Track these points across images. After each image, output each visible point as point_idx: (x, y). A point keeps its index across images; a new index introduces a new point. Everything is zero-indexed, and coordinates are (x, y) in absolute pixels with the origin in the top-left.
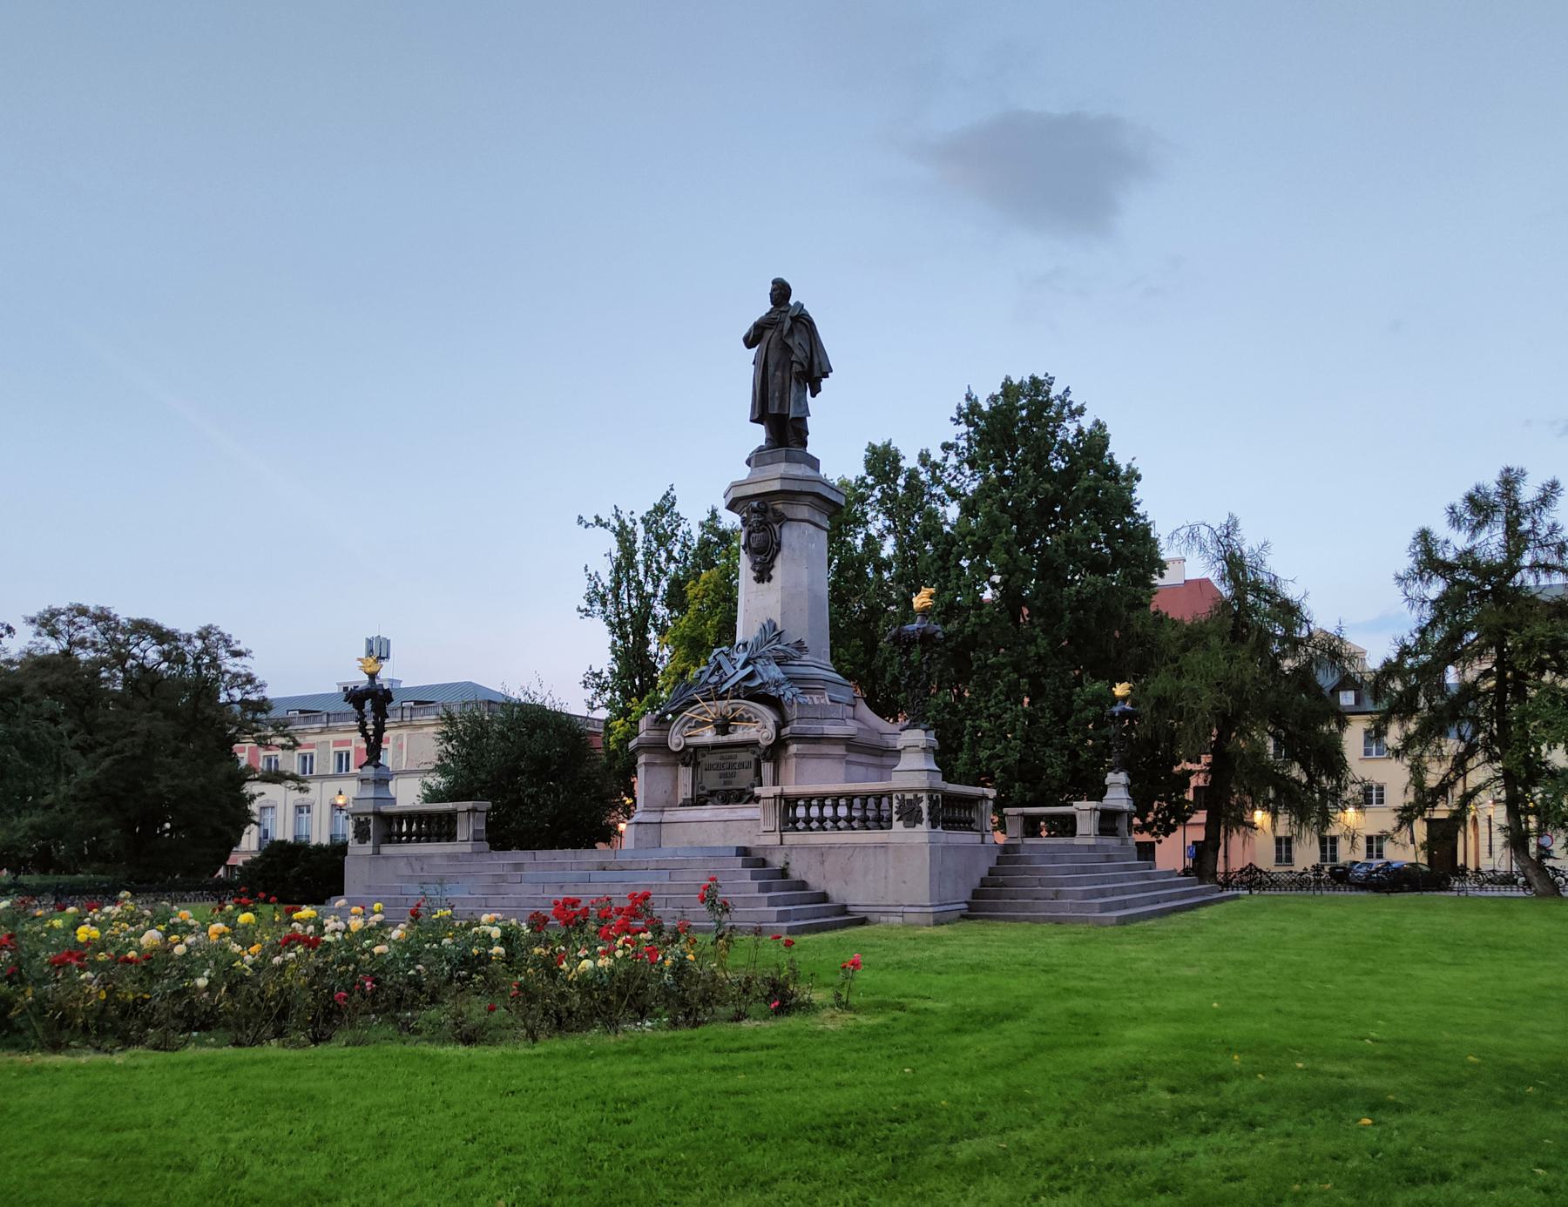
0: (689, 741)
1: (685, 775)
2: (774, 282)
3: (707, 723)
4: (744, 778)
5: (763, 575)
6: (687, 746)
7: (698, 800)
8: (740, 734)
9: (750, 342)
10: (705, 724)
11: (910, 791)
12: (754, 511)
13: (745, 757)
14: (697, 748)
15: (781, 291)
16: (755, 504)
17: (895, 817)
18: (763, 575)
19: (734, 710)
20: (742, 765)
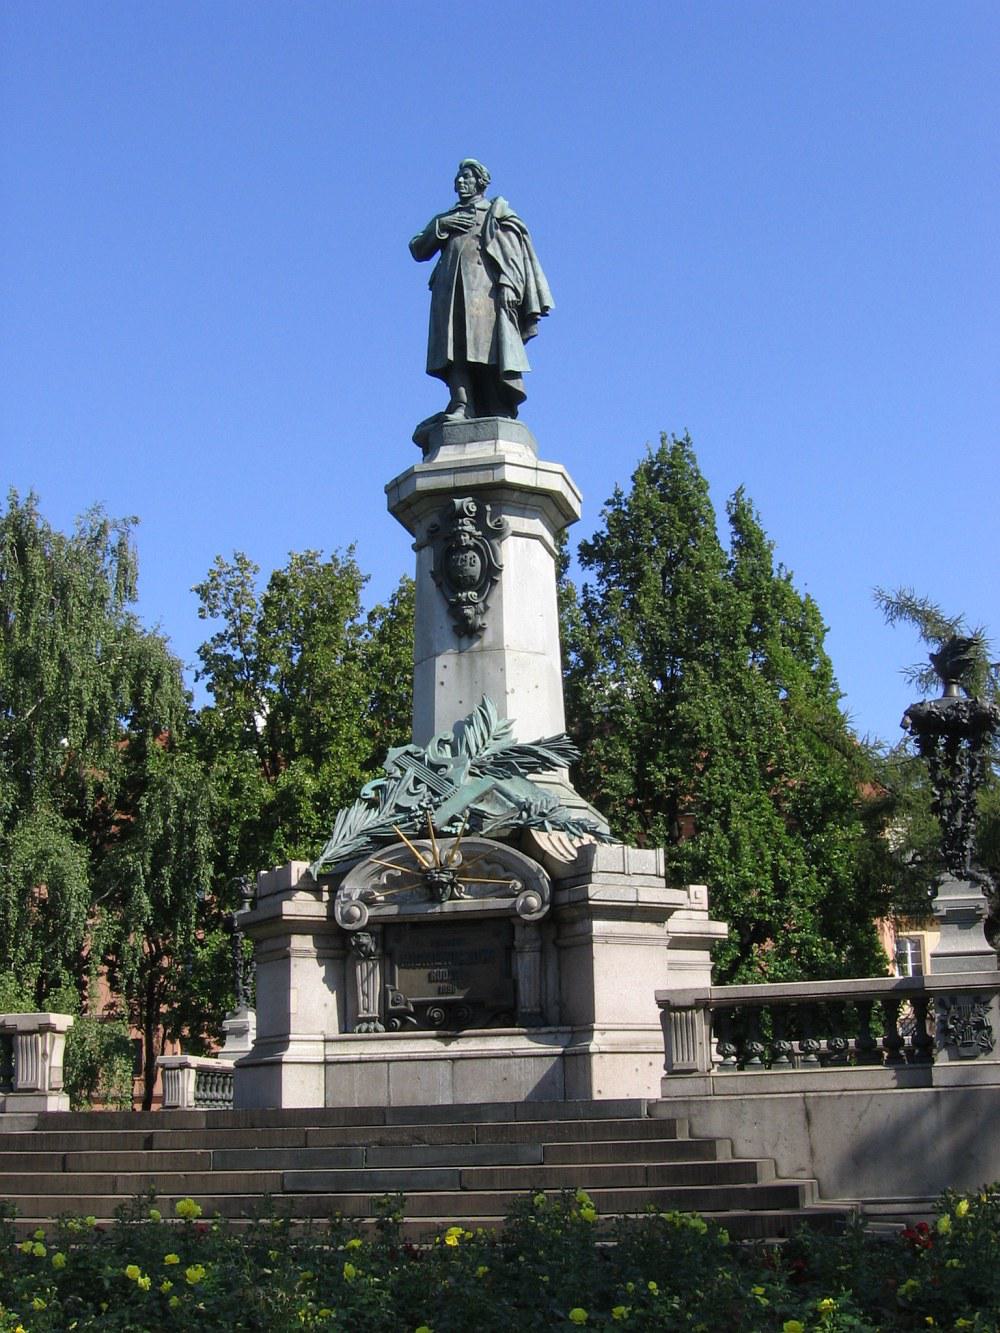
6: (372, 921)
7: (394, 1020)
9: (422, 249)
15: (471, 181)
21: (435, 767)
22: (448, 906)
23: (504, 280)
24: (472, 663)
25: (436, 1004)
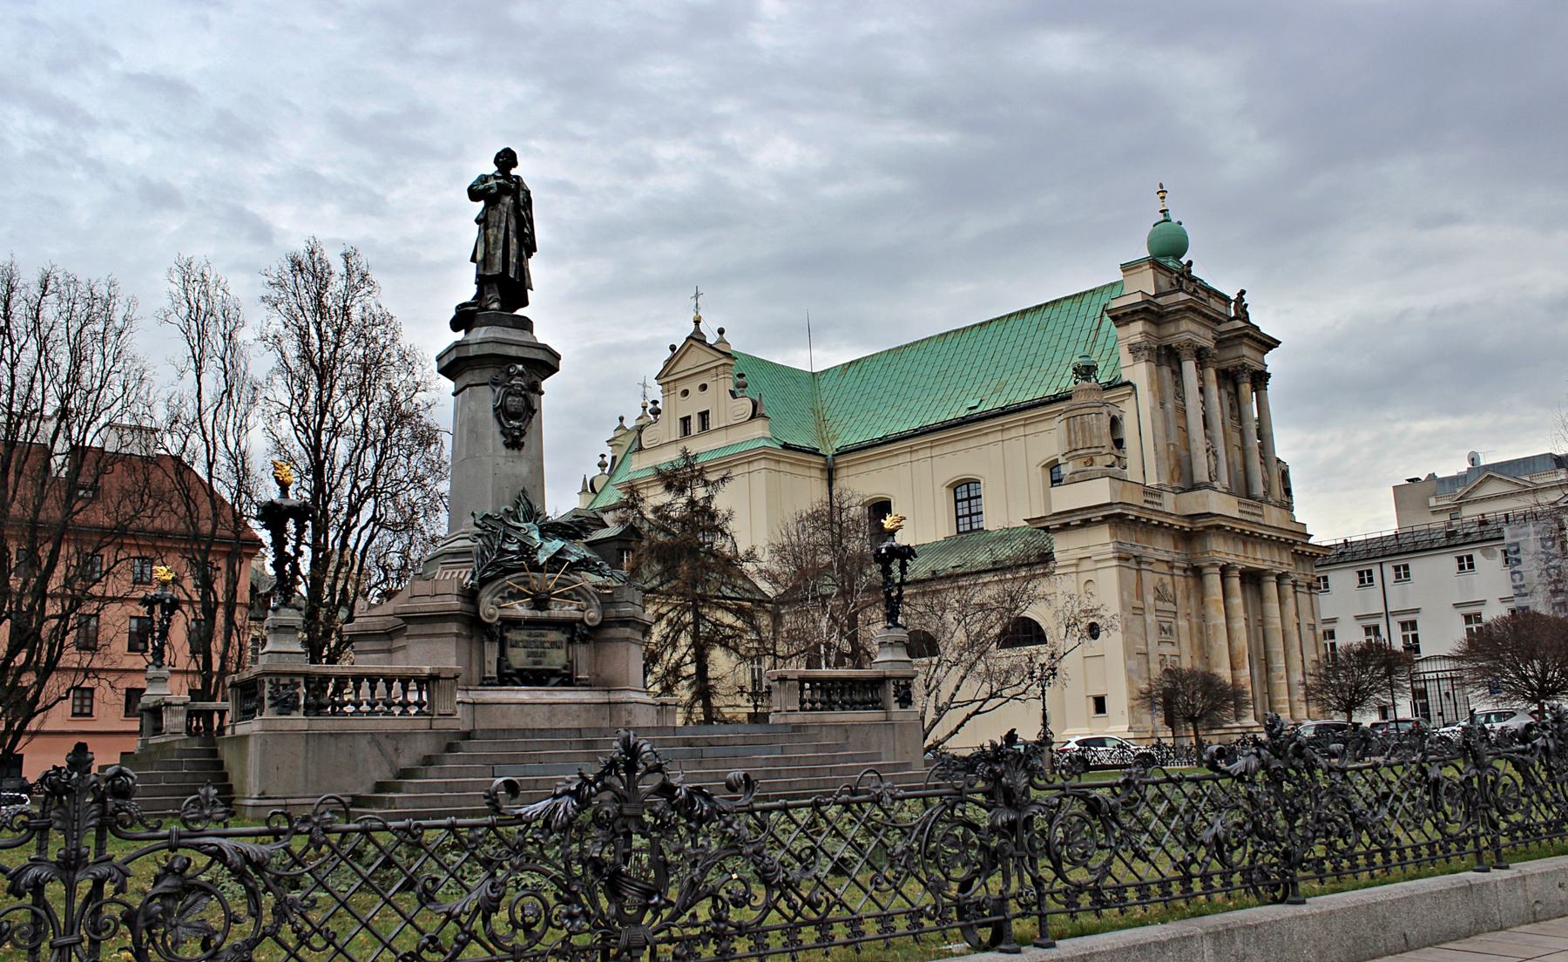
0: (498, 613)
1: (492, 652)
3: (528, 596)
4: (557, 659)
10: (519, 595)
11: (902, 678)
13: (554, 636)
15: (506, 159)
16: (520, 367)
18: (514, 442)
19: (557, 585)
20: (554, 645)
22: (545, 614)
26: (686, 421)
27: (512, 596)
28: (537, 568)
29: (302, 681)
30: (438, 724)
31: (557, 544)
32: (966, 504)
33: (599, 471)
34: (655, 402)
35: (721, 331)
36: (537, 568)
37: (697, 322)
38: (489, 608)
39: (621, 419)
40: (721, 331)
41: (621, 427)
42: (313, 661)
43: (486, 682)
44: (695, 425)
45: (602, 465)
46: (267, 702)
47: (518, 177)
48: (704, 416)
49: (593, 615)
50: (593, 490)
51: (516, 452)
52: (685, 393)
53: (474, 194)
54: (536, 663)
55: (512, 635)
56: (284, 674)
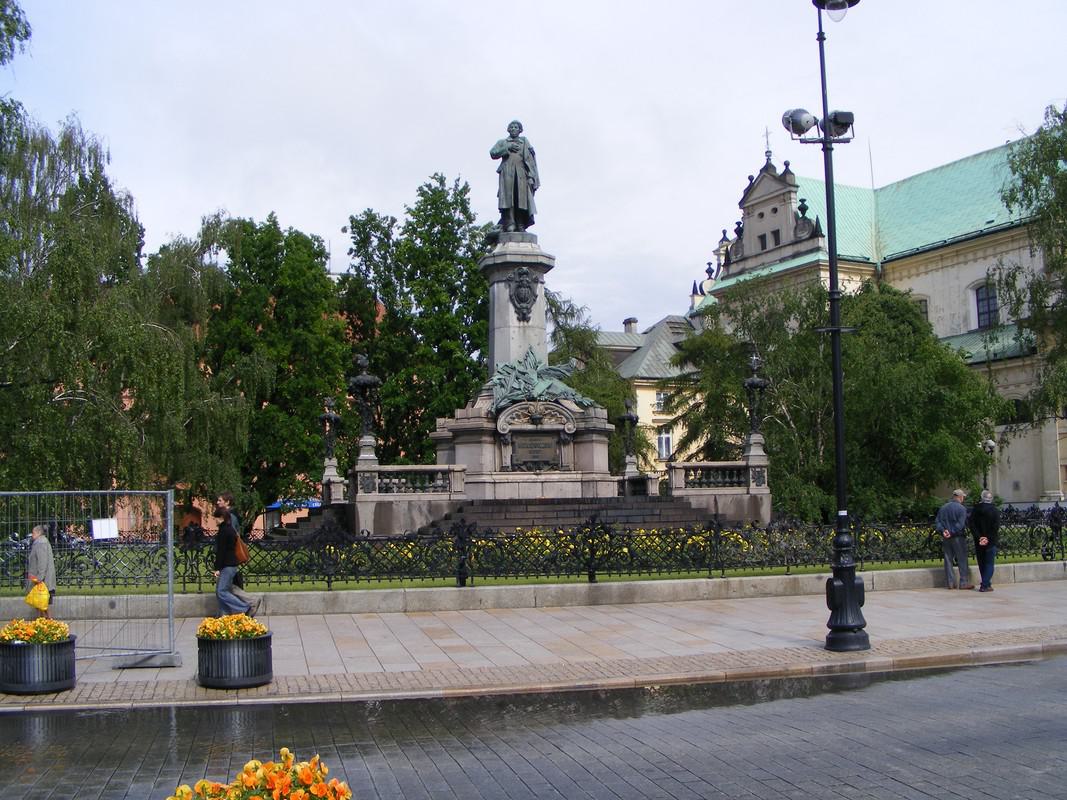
0: (510, 427)
1: (508, 451)
2: (513, 123)
4: (547, 454)
5: (523, 317)
6: (510, 431)
7: (516, 467)
8: (549, 424)
11: (758, 467)
12: (525, 273)
14: (514, 433)
15: (515, 129)
16: (525, 268)
17: (751, 480)
18: (523, 317)
21: (524, 374)
23: (530, 175)
24: (524, 331)
25: (532, 462)
26: (762, 238)
27: (518, 417)
28: (533, 399)
29: (377, 475)
30: (455, 497)
31: (548, 382)
32: (986, 302)
33: (707, 276)
34: (738, 223)
35: (787, 164)
36: (533, 399)
37: (768, 153)
38: (503, 425)
39: (724, 232)
40: (787, 164)
41: (725, 239)
42: (381, 463)
43: (503, 469)
44: (770, 244)
45: (710, 271)
46: (359, 487)
47: (524, 139)
48: (776, 234)
49: (570, 428)
50: (703, 293)
51: (525, 323)
52: (761, 215)
53: (495, 156)
54: (534, 457)
55: (519, 440)
56: (368, 472)
